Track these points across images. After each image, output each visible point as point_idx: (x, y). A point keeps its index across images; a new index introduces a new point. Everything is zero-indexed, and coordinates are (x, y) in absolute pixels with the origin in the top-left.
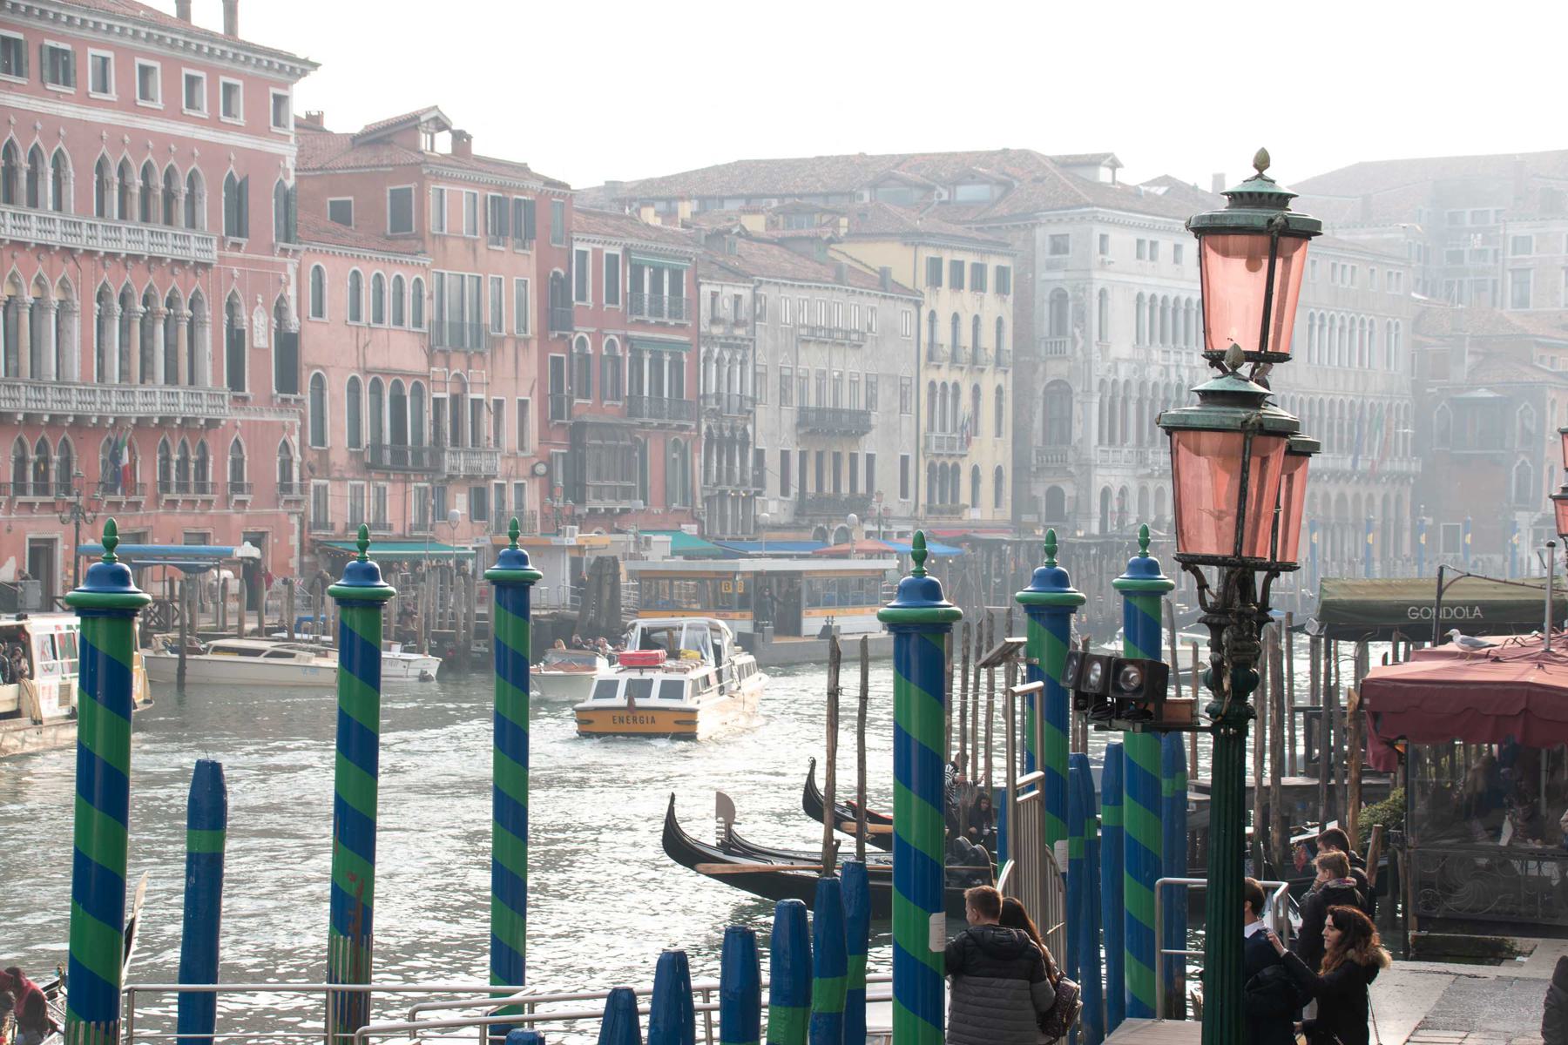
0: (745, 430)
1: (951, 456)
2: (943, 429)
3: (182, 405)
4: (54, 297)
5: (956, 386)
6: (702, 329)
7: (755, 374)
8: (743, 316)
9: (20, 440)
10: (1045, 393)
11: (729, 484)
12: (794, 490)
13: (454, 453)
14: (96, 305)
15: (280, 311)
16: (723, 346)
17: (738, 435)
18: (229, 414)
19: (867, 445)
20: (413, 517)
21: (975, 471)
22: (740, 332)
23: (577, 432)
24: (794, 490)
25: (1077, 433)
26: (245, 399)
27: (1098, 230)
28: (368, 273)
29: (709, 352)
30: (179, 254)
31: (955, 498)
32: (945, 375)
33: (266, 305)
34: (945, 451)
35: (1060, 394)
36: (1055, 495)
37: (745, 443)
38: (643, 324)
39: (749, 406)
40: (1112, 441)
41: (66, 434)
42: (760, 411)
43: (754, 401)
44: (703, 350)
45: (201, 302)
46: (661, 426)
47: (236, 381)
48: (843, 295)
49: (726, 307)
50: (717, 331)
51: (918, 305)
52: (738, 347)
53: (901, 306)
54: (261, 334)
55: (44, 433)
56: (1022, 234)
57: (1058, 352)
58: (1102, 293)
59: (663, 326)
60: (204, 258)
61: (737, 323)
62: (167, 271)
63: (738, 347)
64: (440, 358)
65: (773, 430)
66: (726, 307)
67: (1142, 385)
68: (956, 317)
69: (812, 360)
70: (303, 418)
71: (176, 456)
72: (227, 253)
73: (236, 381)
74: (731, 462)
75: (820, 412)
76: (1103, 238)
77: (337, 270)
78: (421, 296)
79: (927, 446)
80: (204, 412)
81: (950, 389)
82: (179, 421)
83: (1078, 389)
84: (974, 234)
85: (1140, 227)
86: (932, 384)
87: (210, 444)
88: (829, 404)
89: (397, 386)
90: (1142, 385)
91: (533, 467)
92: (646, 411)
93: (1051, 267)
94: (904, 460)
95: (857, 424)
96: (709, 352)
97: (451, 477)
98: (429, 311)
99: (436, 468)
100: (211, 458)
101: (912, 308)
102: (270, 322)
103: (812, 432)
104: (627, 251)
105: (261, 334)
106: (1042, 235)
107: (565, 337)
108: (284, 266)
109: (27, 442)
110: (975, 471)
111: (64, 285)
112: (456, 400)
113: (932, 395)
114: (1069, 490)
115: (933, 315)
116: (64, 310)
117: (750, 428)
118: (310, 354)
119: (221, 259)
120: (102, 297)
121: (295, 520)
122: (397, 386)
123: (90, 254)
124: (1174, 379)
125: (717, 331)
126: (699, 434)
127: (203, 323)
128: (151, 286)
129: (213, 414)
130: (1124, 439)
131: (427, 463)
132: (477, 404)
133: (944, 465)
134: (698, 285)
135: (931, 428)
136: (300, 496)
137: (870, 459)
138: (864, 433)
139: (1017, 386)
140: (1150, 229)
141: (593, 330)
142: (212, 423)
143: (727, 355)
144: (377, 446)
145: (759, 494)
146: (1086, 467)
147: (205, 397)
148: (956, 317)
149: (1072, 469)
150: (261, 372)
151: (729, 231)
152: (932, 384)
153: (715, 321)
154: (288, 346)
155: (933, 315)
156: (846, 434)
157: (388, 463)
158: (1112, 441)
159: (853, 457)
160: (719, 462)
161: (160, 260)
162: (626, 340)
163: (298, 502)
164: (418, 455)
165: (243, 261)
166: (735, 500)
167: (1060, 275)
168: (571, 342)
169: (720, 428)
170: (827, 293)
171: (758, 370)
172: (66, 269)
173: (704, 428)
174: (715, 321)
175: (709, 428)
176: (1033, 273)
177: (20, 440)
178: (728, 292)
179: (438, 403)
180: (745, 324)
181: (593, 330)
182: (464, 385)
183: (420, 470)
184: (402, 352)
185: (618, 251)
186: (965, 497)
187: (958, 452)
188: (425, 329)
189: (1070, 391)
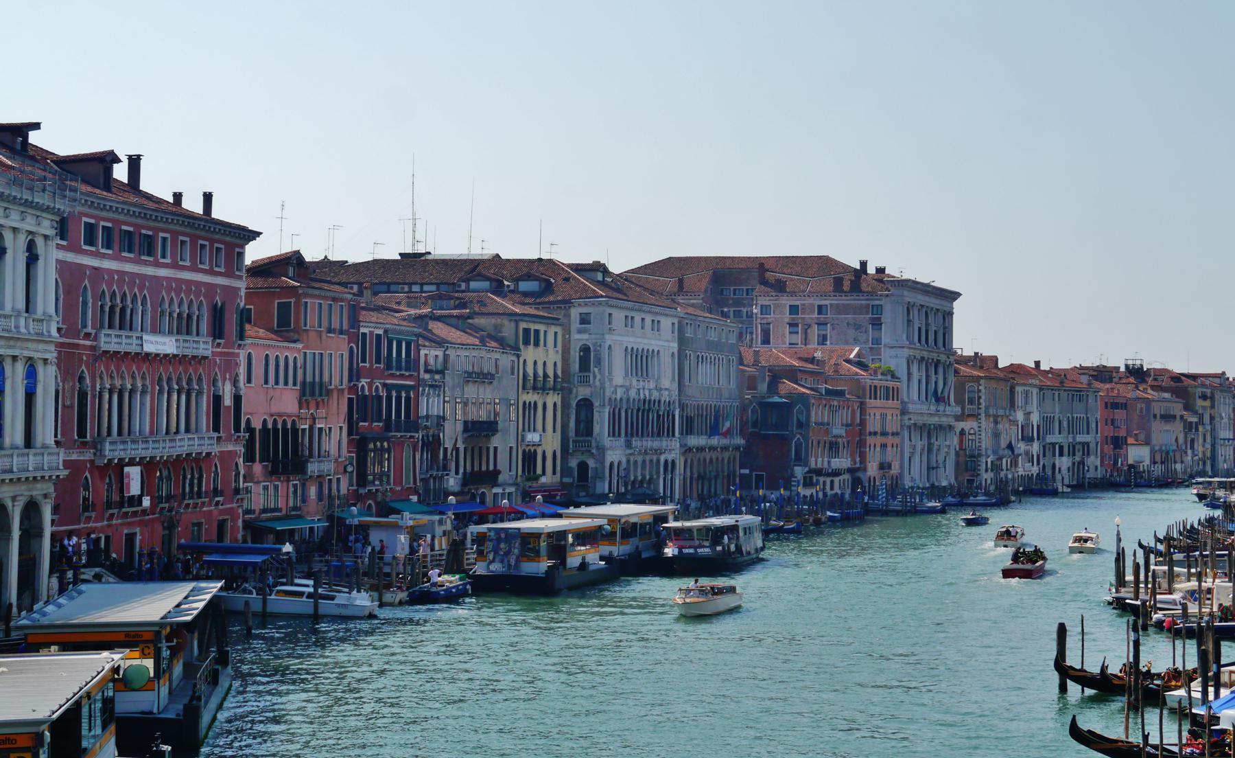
5: (535, 403)
12: (461, 471)
19: (496, 441)
24: (461, 471)
25: (596, 429)
27: (609, 310)
32: (530, 397)
35: (586, 406)
36: (583, 466)
38: (393, 376)
57: (585, 381)
58: (610, 347)
65: (452, 435)
67: (628, 400)
68: (535, 363)
76: (610, 315)
83: (596, 404)
85: (627, 308)
90: (628, 400)
93: (580, 332)
106: (575, 313)
114: (591, 463)
115: (525, 361)
137: (496, 448)
140: (632, 309)
146: (602, 450)
148: (535, 363)
149: (594, 451)
155: (525, 361)
162: (385, 385)
167: (586, 336)
185: (381, 332)
186: (539, 471)
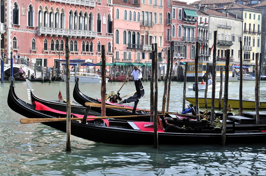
0: (207, 44)
1: (249, 50)
2: (247, 45)
3: (86, 34)
4: (60, 12)
5: (250, 37)
6: (198, 25)
7: (209, 33)
8: (207, 22)
9: (52, 40)
11: (204, 54)
13: (145, 46)
14: (69, 14)
15: (109, 16)
16: (202, 28)
17: (205, 45)
18: (97, 36)
20: (136, 58)
22: (207, 25)
23: (172, 43)
26: (101, 34)
28: (128, 11)
29: (200, 29)
30: (87, 5)
31: (249, 58)
33: (106, 16)
34: (247, 49)
37: (207, 46)
38: (186, 23)
39: (208, 40)
41: (62, 39)
42: (210, 41)
43: (209, 39)
44: (198, 28)
45: (92, 14)
46: (190, 43)
47: (99, 30)
48: (227, 19)
49: (203, 21)
50: (202, 25)
51: (242, 22)
52: (206, 28)
53: (239, 22)
54: (104, 21)
55: (57, 39)
56: (264, 9)
59: (190, 24)
60: (92, 6)
61: (206, 23)
62: (85, 8)
64: (143, 27)
66: (203, 21)
70: (113, 38)
71: (86, 44)
72: (98, 5)
73: (99, 30)
74: (204, 50)
77: (122, 10)
78: (139, 16)
79: (244, 48)
80: (91, 36)
81: (246, 38)
82: (86, 37)
84: (254, 9)
86: (245, 37)
87: (93, 42)
88: (224, 40)
89: (134, 32)
91: (162, 49)
92: (186, 40)
96: (200, 29)
97: (145, 51)
98: (141, 18)
99: (142, 49)
100: (93, 45)
101: (241, 22)
102: (106, 19)
103: (221, 45)
104: (183, 9)
105: (104, 21)
107: (170, 25)
108: (110, 8)
109: (54, 40)
111: (62, 10)
112: (147, 36)
113: (245, 39)
115: (245, 24)
116: (62, 15)
117: (208, 44)
118: (116, 26)
119: (96, 6)
120: (70, 13)
121: (111, 58)
122: (134, 32)
123: (68, 4)
125: (202, 25)
127: (92, 19)
128: (81, 11)
129: (93, 36)
131: (140, 48)
132: (151, 37)
133: (247, 52)
135: (245, 45)
136: (112, 53)
137: (232, 50)
138: (231, 45)
139: (262, 37)
141: (176, 24)
142: (93, 38)
143: (203, 30)
144: (129, 45)
145: (209, 56)
147: (93, 33)
148: (250, 24)
150: (105, 29)
151: (205, 7)
152: (245, 37)
153: (201, 23)
154: (110, 24)
155: (245, 24)
156: (228, 45)
157: (132, 47)
160: (202, 50)
161: (83, 6)
163: (112, 54)
164: (138, 46)
165: (101, 7)
166: (204, 57)
168: (171, 26)
170: (224, 19)
171: (210, 33)
172: (63, 7)
174: (201, 23)
177: (52, 40)
178: (204, 18)
179: (143, 36)
180: (207, 23)
181: (176, 24)
182: (148, 33)
183: (138, 49)
184: (136, 27)
187: (250, 49)
188: (140, 22)
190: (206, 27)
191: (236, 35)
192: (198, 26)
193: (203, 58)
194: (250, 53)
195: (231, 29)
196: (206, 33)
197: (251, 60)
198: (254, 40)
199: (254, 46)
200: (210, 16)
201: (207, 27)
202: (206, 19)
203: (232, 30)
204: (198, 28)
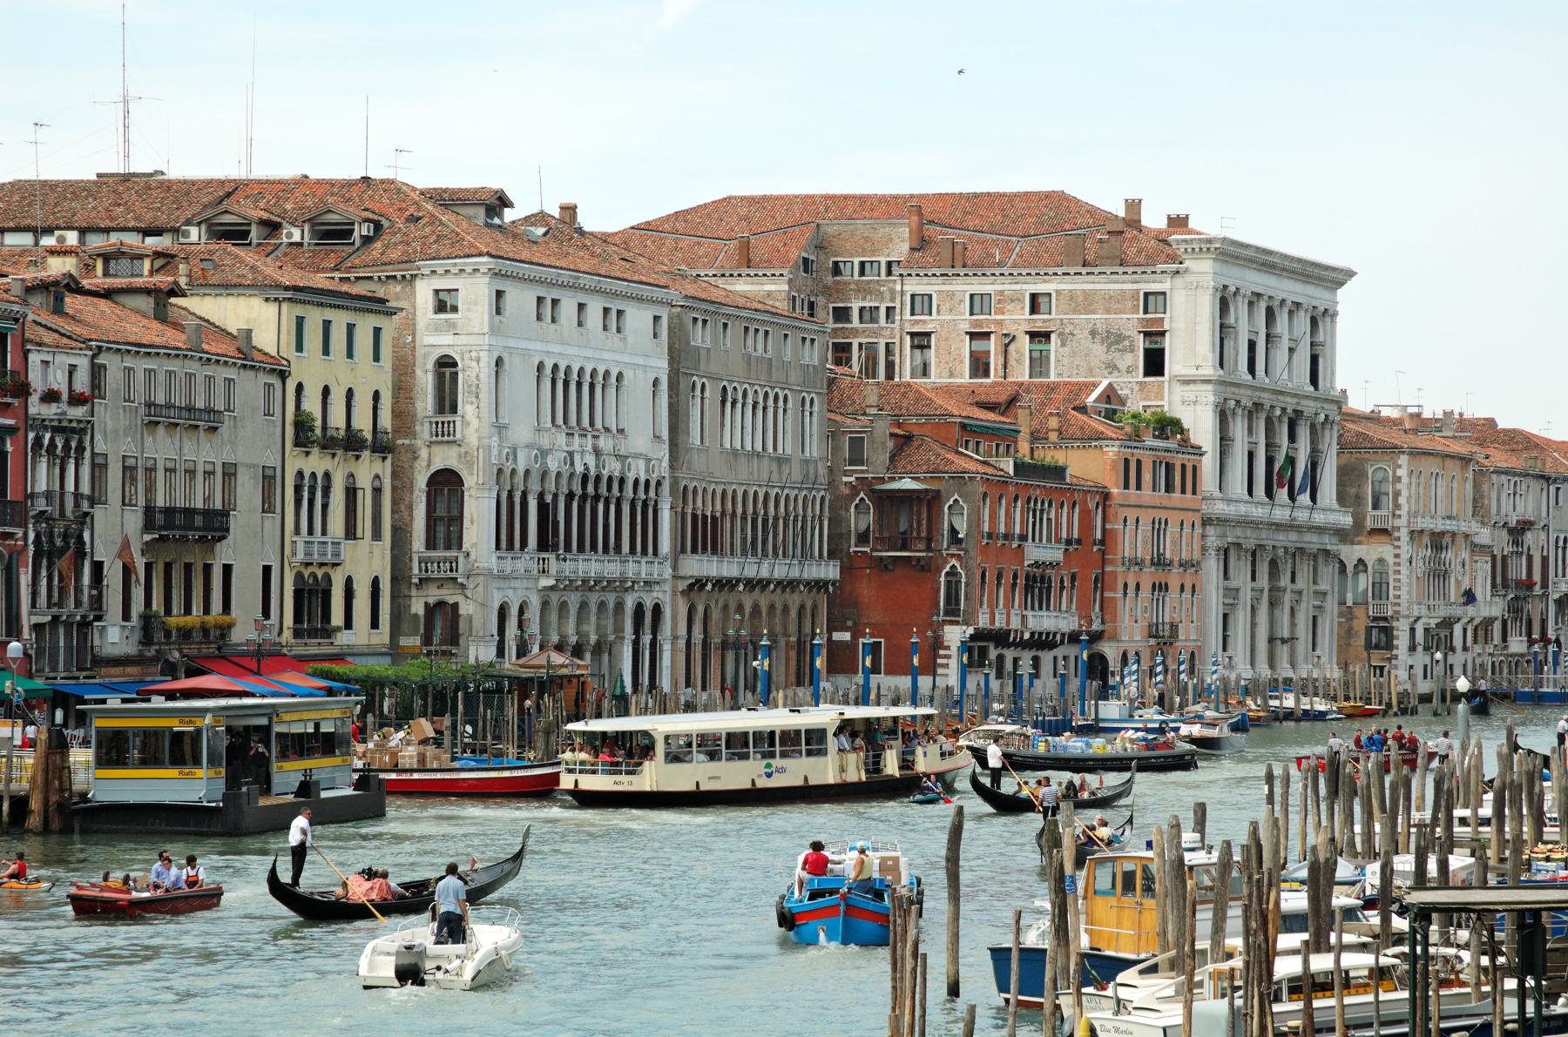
0: (80, 538)
1: (322, 565)
2: (311, 532)
5: (327, 475)
10: (429, 484)
19: (224, 553)
21: (349, 582)
29: (38, 441)
31: (326, 616)
37: (80, 554)
40: (510, 547)
44: (31, 435)
63: (73, 430)
67: (544, 475)
68: (326, 391)
69: (162, 447)
75: (169, 511)
85: (540, 282)
86: (300, 474)
88: (180, 504)
90: (544, 475)
93: (437, 329)
94: (267, 570)
95: (215, 524)
106: (423, 293)
110: (349, 582)
113: (298, 489)
117: (86, 536)
124: (579, 469)
126: (26, 545)
130: (524, 544)
133: (314, 575)
134: (26, 353)
137: (227, 569)
145: (99, 618)
152: (300, 474)
158: (510, 547)
159: (207, 569)
166: (68, 625)
169: (51, 535)
173: (31, 536)
175: (38, 536)
176: (414, 335)
186: (337, 618)
187: (329, 558)
189: (460, 482)
190: (74, 424)
191: (249, 466)
192: (28, 422)
193: (61, 631)
194: (327, 578)
195: (216, 429)
196: (72, 461)
197: (338, 629)
198: (351, 493)
199: (351, 533)
200: (100, 348)
201: (79, 422)
202: (72, 369)
203: (226, 436)
204: (31, 435)
